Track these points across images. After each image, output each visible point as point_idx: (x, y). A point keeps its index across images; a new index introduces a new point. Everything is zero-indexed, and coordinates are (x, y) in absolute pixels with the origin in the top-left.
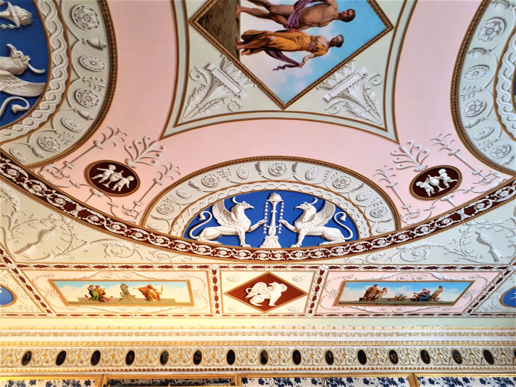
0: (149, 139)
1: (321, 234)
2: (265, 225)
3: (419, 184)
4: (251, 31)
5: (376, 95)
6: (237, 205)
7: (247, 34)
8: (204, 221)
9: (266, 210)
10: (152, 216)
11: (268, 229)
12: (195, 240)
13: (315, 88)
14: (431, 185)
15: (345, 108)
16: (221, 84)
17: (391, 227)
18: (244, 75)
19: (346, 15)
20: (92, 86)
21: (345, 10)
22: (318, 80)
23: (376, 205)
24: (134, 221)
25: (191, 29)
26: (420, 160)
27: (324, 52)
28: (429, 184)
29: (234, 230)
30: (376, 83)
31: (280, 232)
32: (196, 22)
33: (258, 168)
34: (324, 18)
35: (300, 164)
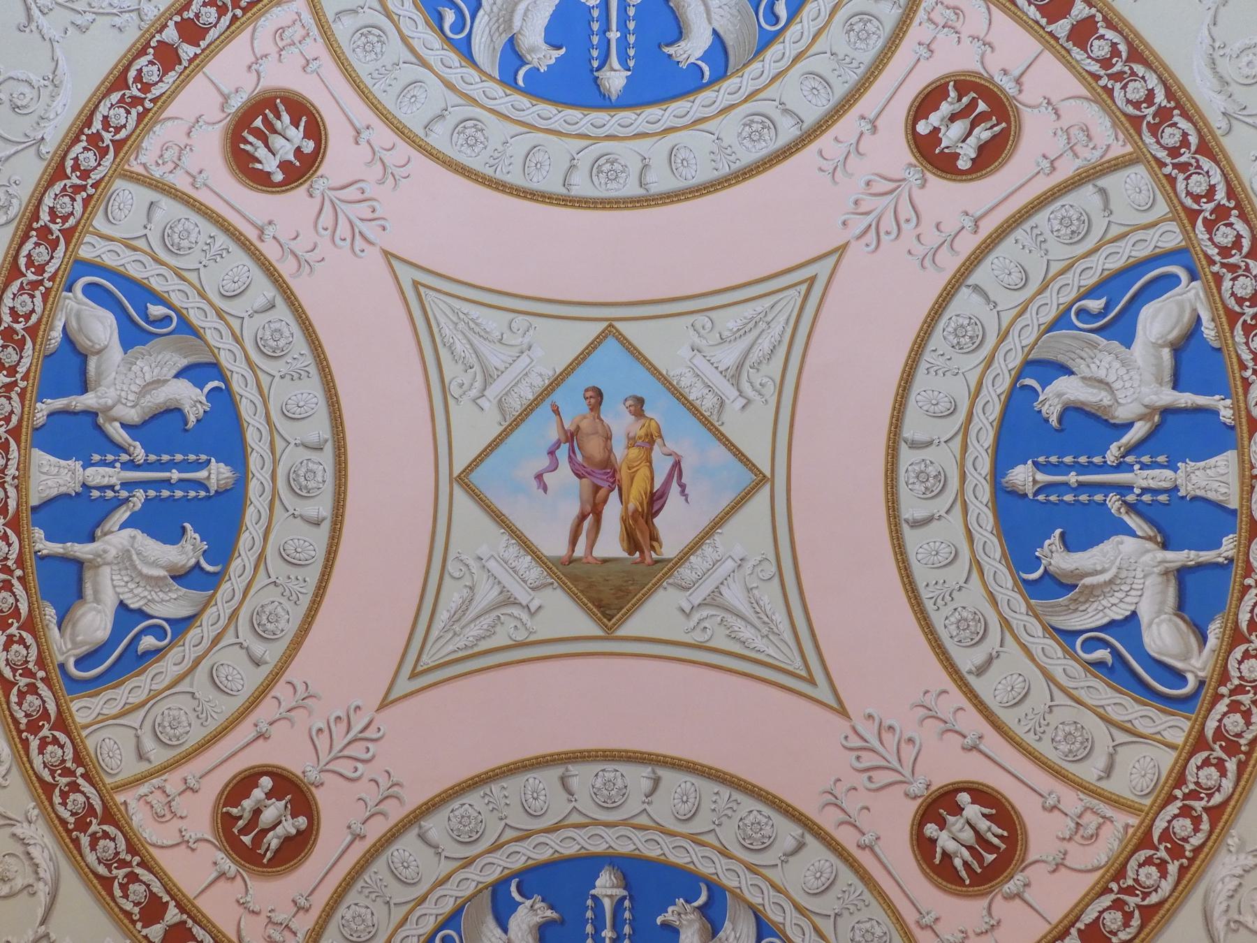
0: (846, 737)
1: (1166, 353)
2: (1131, 498)
4: (622, 540)
5: (729, 320)
6: (1051, 568)
7: (625, 544)
8: (1115, 652)
9: (1068, 498)
10: (1100, 779)
11: (1145, 490)
12: (1202, 683)
13: (721, 428)
16: (717, 591)
17: (1138, 176)
18: (699, 552)
19: (593, 401)
20: (729, 812)
21: (585, 403)
22: (705, 425)
24: (1120, 826)
25: (621, 632)
26: (893, 185)
27: (653, 423)
28: (964, 141)
29: (1153, 582)
30: (709, 325)
31: (1161, 459)
32: (610, 624)
33: (917, 524)
34: (597, 433)
35: (908, 432)
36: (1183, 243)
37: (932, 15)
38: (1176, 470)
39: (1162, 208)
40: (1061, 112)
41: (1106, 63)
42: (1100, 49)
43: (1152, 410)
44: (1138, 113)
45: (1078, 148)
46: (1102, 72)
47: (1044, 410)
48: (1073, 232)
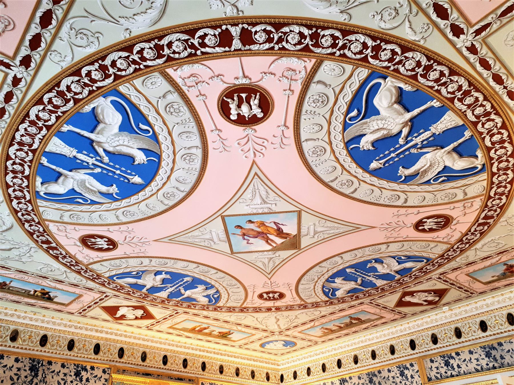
1: (396, 106)
3: (260, 115)
14: (251, 106)
15: (269, 196)
23: (312, 113)
26: (246, 139)
28: (251, 109)
36: (370, 71)
37: (188, 85)
38: (430, 130)
39: (349, 68)
40: (273, 72)
41: (269, 40)
42: (261, 37)
43: (405, 124)
44: (303, 45)
45: (293, 78)
46: (272, 45)
47: (365, 148)
48: (322, 102)
